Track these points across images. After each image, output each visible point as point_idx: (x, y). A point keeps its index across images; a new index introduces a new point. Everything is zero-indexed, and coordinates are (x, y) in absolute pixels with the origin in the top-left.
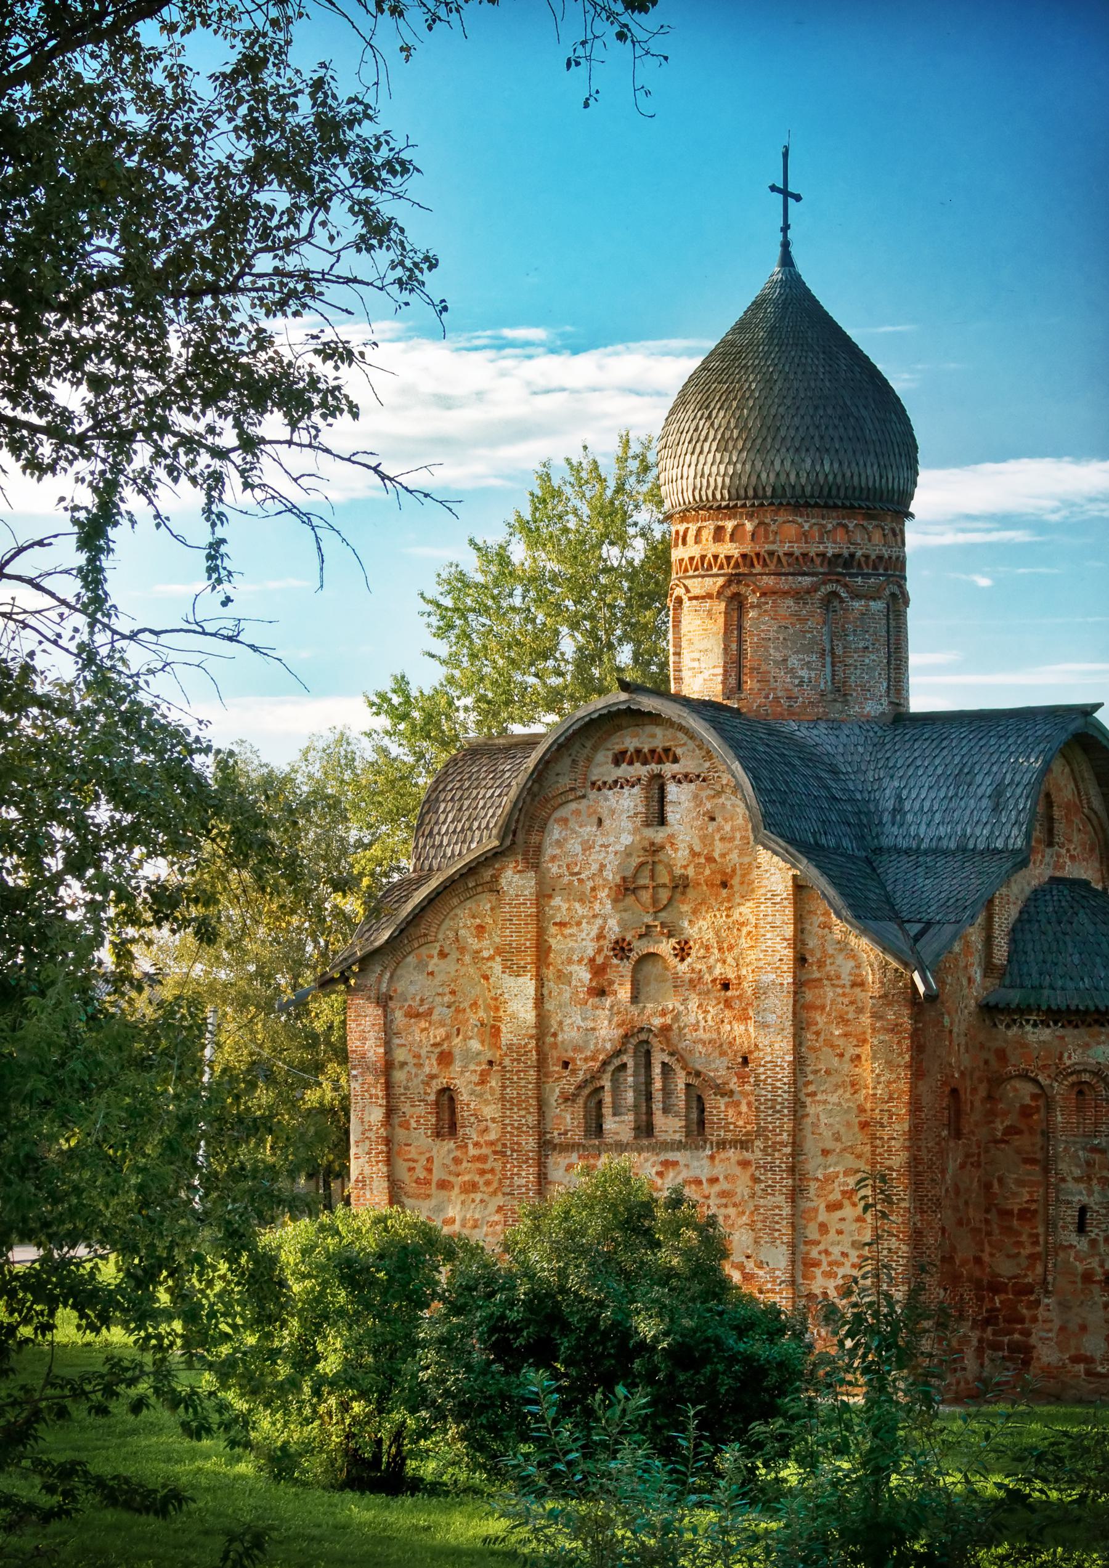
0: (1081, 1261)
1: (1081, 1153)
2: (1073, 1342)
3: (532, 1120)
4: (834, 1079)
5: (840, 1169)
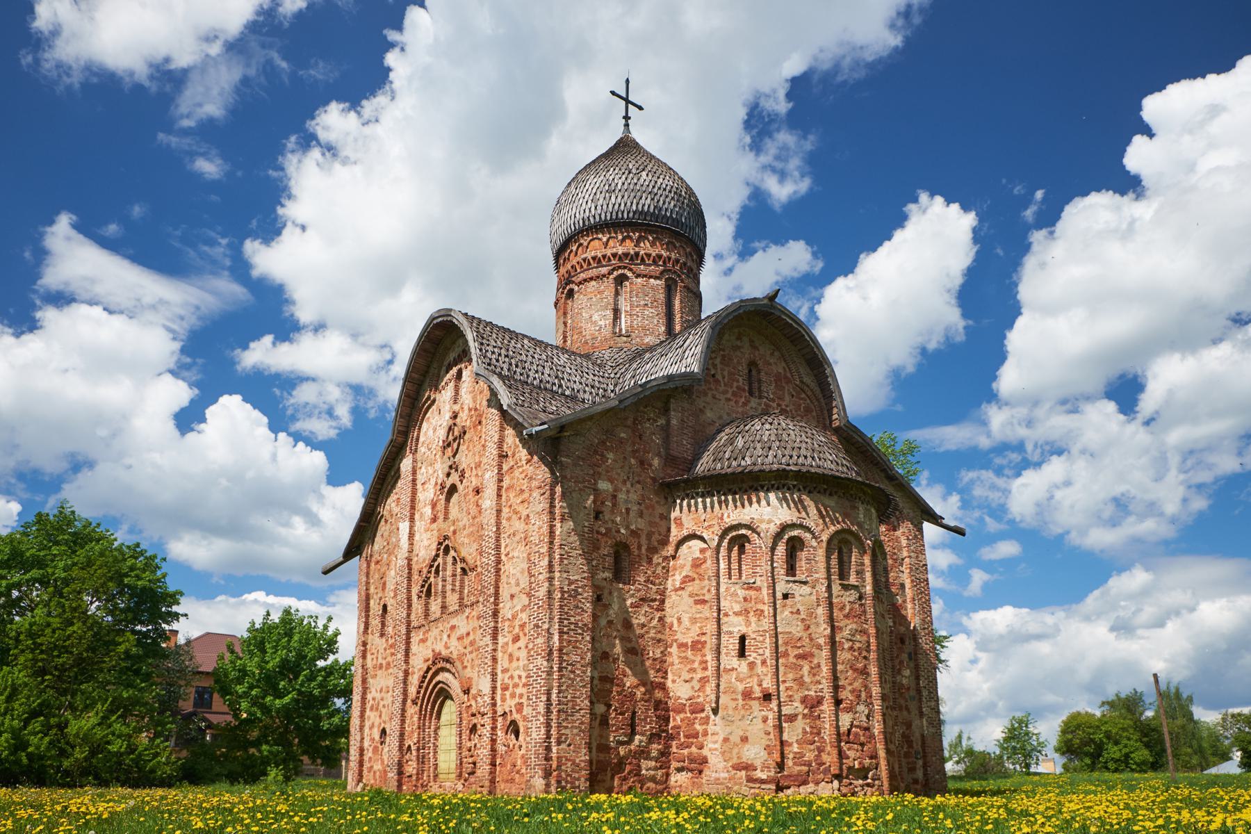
0: (741, 681)
1: (739, 592)
2: (735, 751)
3: (404, 614)
4: (517, 538)
5: (519, 608)
